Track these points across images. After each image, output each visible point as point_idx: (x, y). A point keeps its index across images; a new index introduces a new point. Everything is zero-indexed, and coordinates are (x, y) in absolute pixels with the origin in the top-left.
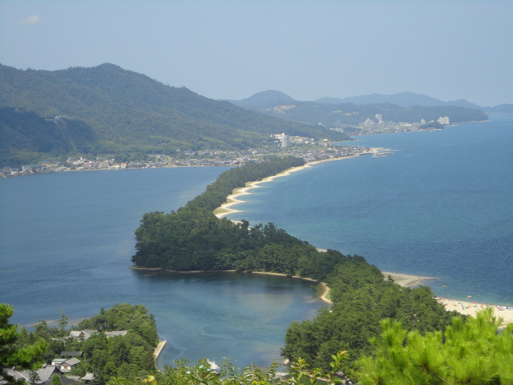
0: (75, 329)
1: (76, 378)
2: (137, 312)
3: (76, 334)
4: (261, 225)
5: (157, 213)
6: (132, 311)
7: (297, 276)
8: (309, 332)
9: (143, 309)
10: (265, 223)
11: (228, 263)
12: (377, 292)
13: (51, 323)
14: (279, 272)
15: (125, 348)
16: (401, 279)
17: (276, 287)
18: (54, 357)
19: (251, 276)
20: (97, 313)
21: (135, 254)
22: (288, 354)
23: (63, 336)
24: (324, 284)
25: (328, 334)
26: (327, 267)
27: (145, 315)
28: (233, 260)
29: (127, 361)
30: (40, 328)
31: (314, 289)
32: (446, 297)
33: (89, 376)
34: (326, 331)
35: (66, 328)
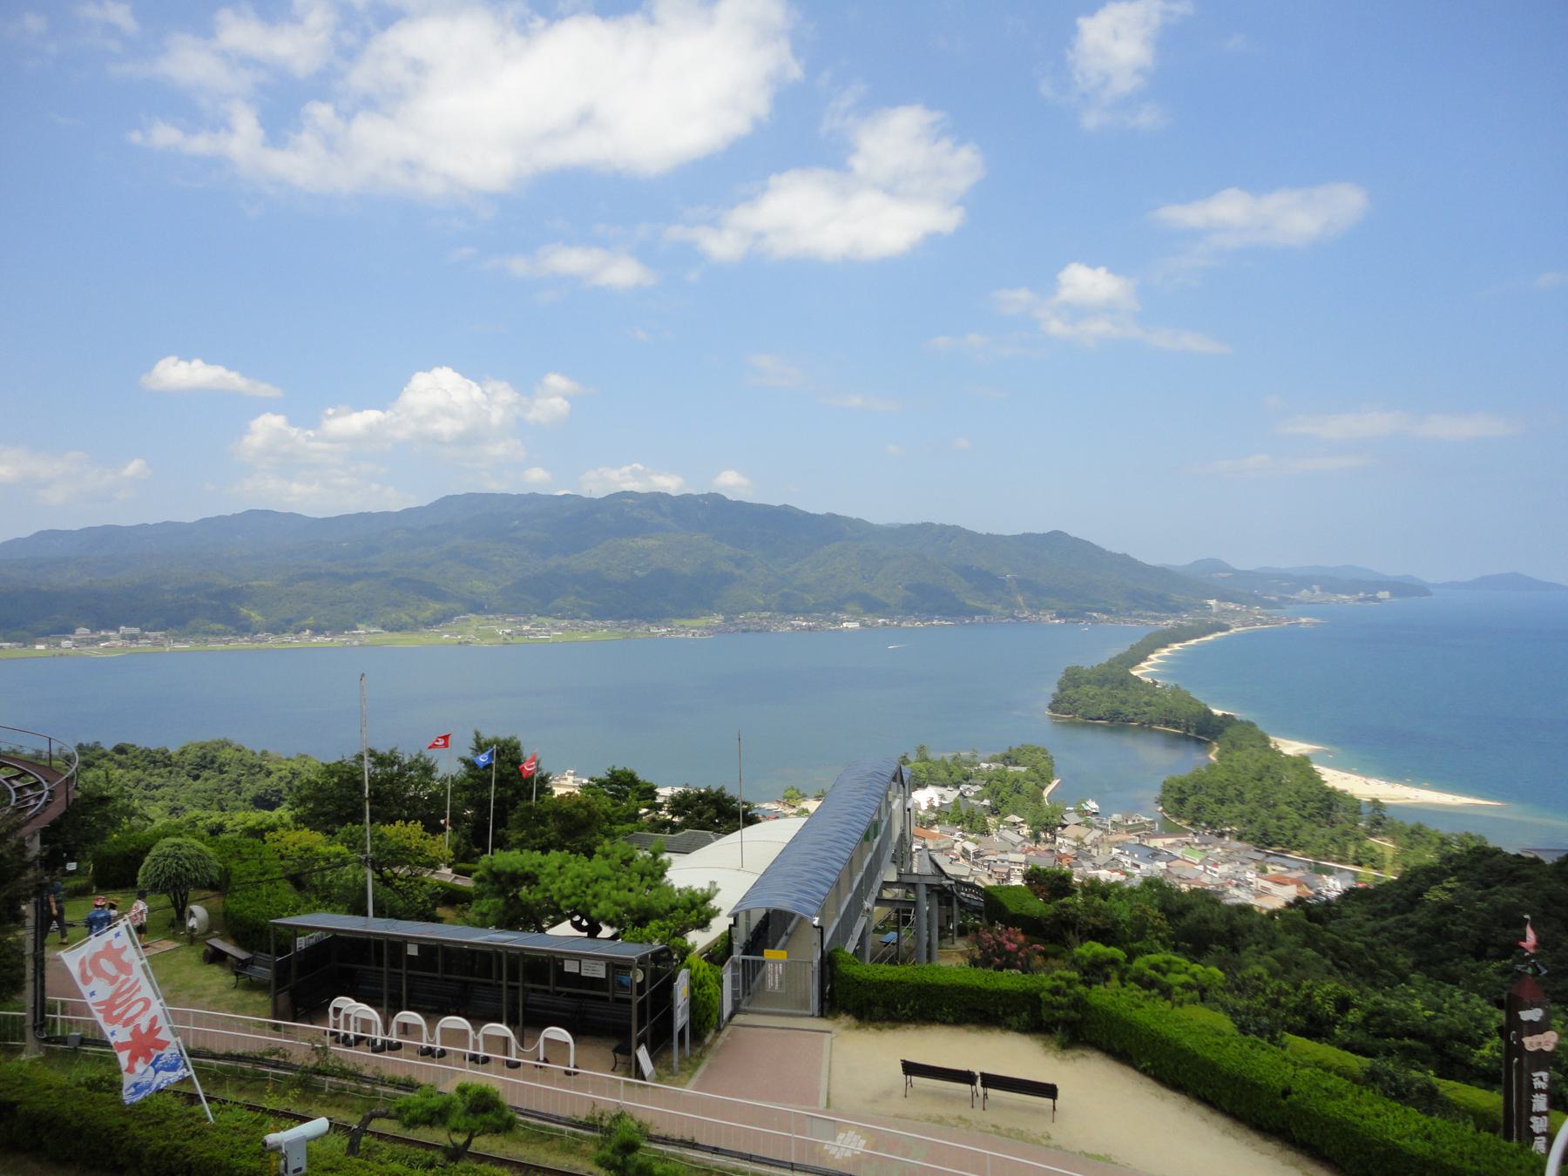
3: (984, 765)
6: (1035, 751)
10: (1172, 683)
13: (965, 754)
19: (1151, 730)
20: (1006, 751)
22: (1161, 801)
25: (1196, 788)
33: (986, 802)
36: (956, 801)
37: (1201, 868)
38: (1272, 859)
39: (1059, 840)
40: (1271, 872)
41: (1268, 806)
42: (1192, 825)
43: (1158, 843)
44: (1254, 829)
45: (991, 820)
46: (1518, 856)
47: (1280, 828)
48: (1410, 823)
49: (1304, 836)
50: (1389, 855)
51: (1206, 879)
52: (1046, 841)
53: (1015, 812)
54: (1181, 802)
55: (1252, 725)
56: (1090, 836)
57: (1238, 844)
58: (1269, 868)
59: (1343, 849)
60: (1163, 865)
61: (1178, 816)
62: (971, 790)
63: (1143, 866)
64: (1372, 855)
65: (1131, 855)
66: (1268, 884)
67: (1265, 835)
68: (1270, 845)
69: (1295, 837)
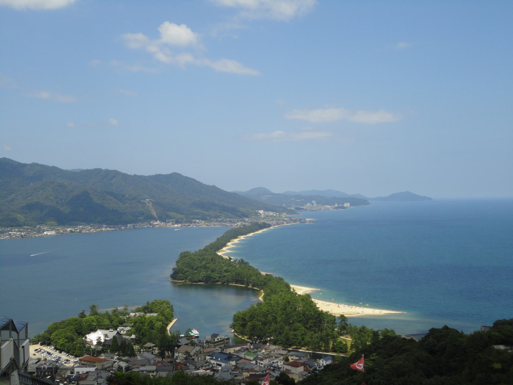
0: (133, 312)
1: (127, 337)
2: (165, 304)
3: (132, 314)
4: (237, 260)
5: (187, 252)
6: (162, 303)
7: (250, 287)
8: (243, 316)
9: (168, 302)
10: (239, 258)
11: (217, 279)
12: (283, 297)
13: (121, 308)
14: (242, 284)
15: (152, 322)
16: (301, 289)
17: (239, 291)
18: (118, 326)
19: (228, 286)
20: (145, 304)
21: (172, 273)
22: (233, 326)
23: (125, 315)
24: (262, 291)
25: (252, 317)
26: (264, 283)
27: (168, 306)
28: (220, 277)
29: (153, 329)
30: (114, 311)
31: (256, 293)
32: (319, 299)
33: (133, 336)
34: (251, 316)
35: (128, 311)
36: (114, 337)
37: (254, 362)
38: (291, 353)
39: (176, 355)
40: (291, 361)
41: (289, 324)
42: (249, 338)
43: (231, 351)
44: (282, 338)
45: (136, 347)
46: (404, 339)
47: (295, 335)
48: (359, 326)
49: (307, 339)
50: (349, 345)
51: (257, 369)
52: (168, 357)
53: (150, 341)
54: (244, 326)
55: (282, 279)
56: (193, 351)
57: (273, 347)
58: (290, 358)
59: (327, 343)
60: (233, 363)
61: (242, 334)
62: (123, 330)
63: (223, 365)
64: (341, 345)
65: (217, 359)
66: (289, 367)
67: (288, 340)
68: (290, 346)
69: (303, 339)
